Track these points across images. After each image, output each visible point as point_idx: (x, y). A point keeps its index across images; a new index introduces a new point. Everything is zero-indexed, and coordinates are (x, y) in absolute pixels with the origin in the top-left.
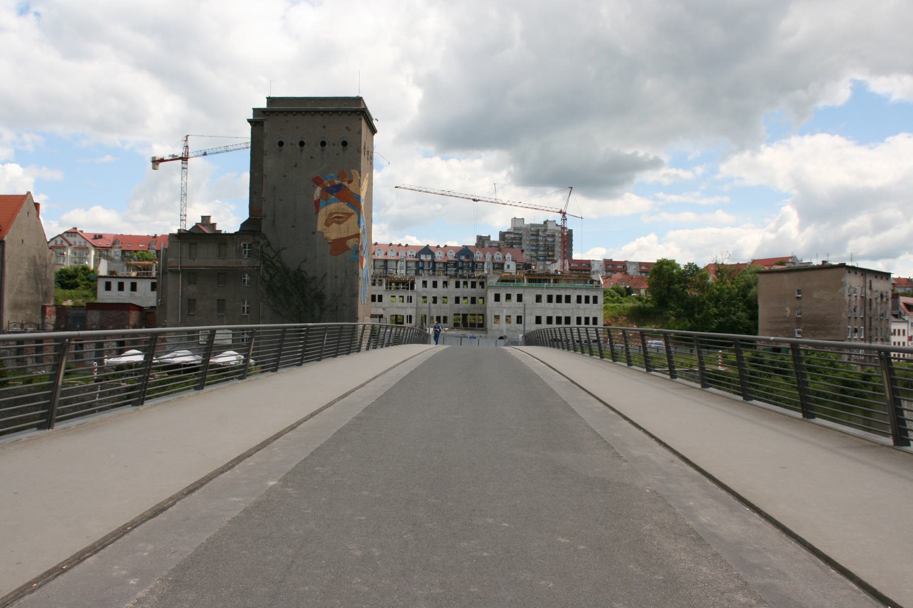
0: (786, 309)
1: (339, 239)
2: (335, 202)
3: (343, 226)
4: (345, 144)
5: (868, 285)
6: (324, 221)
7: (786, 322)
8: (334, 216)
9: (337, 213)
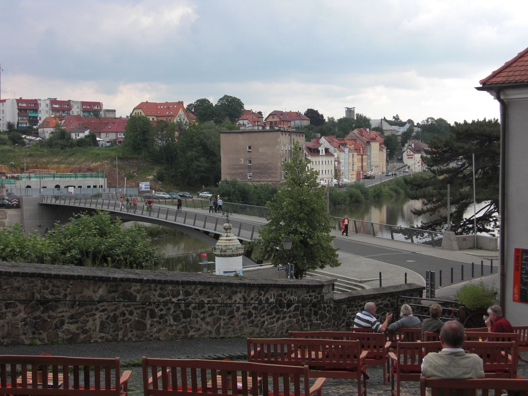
0: (241, 159)
5: (292, 142)
7: (241, 168)
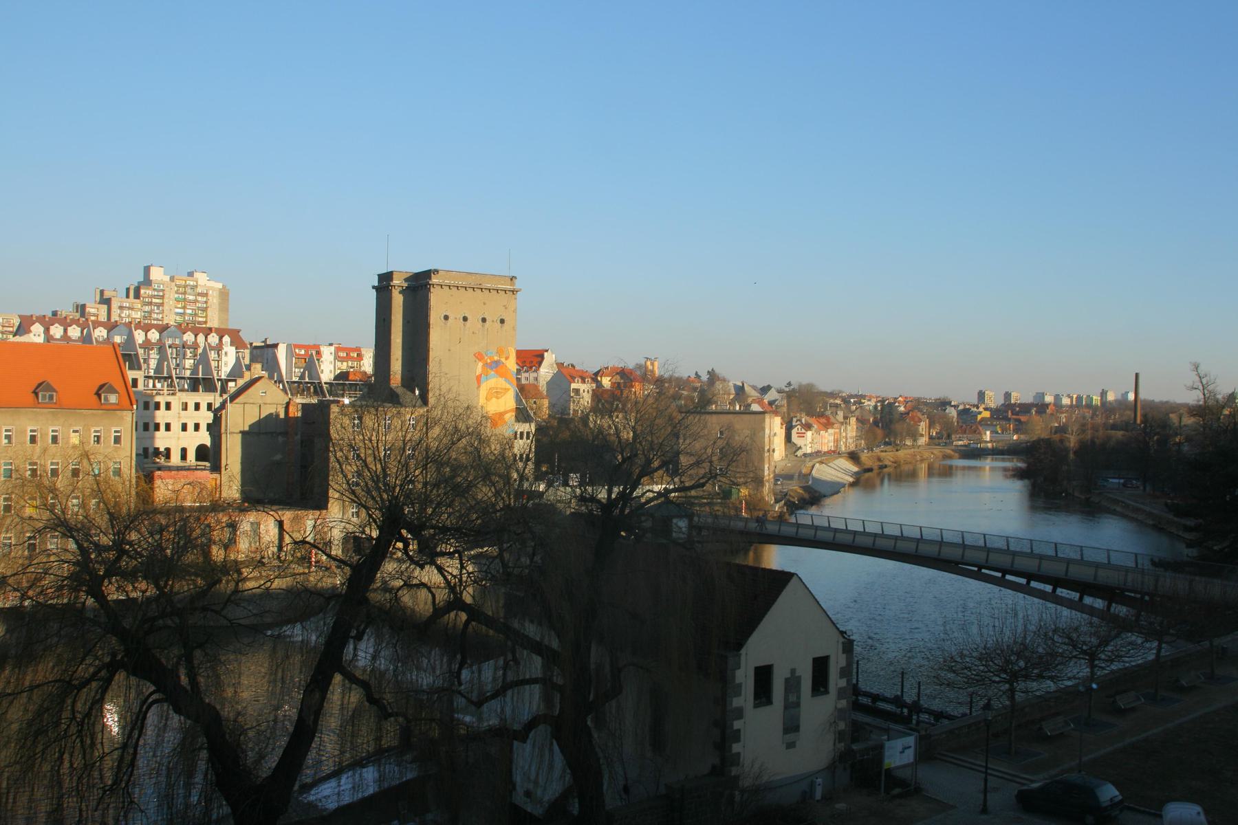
3: (502, 401)
4: (502, 321)
9: (497, 388)
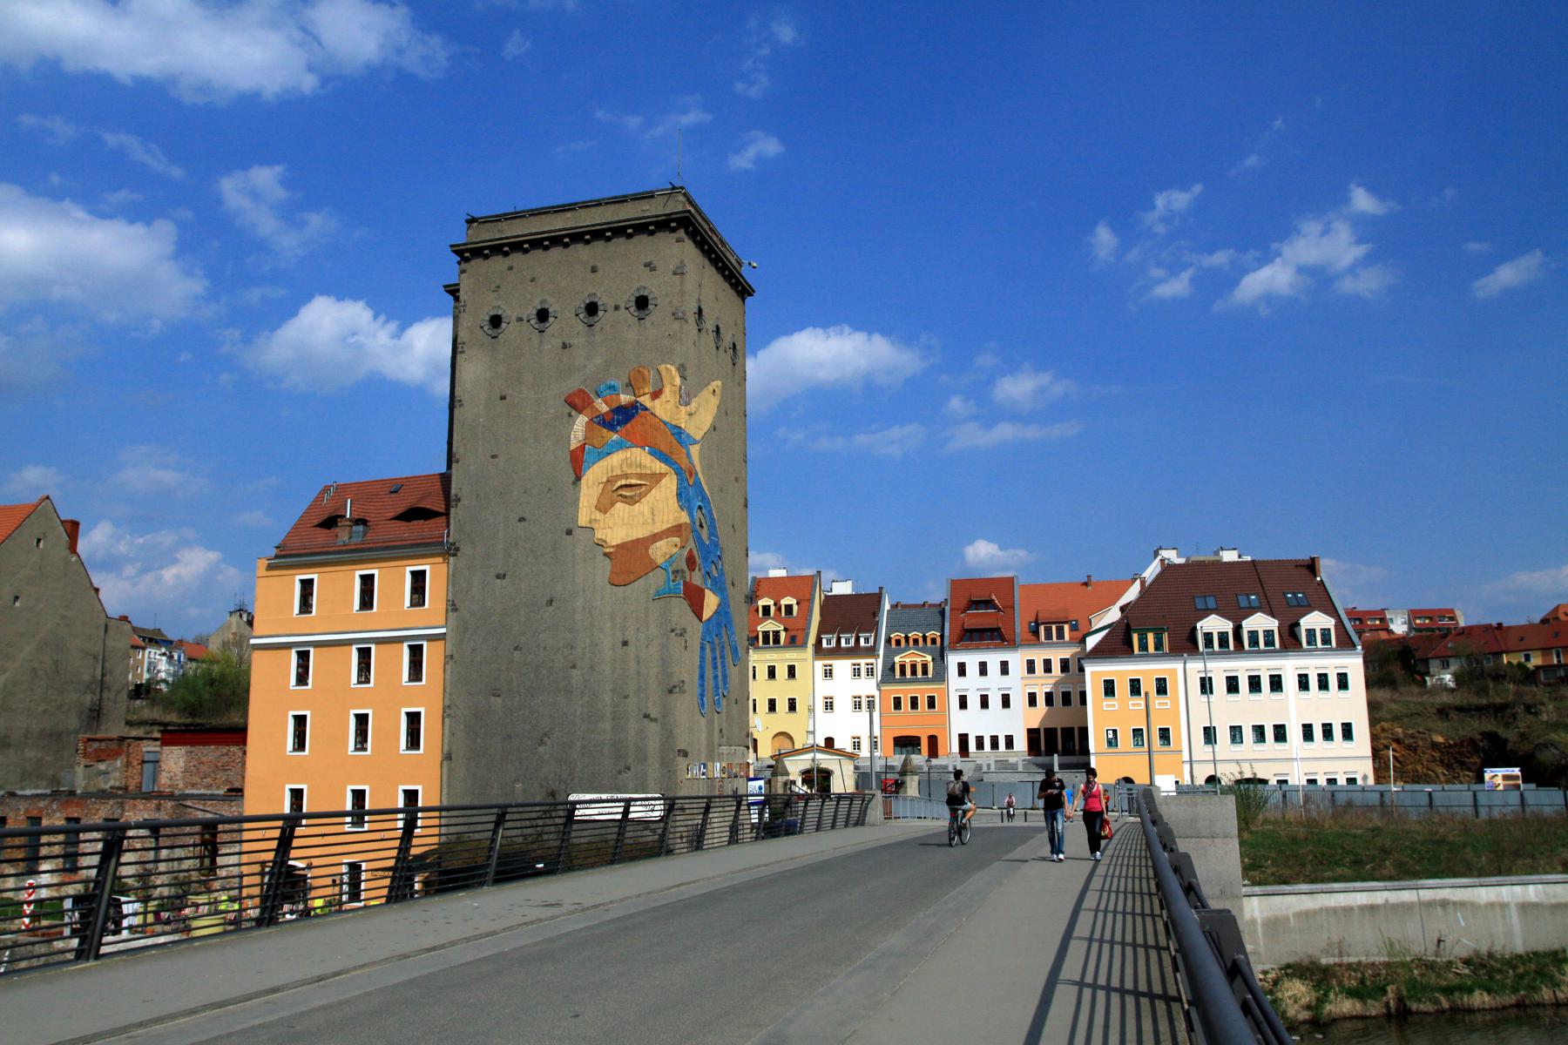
1: (633, 541)
2: (621, 448)
3: (643, 507)
6: (595, 502)
8: (619, 484)
9: (626, 476)
